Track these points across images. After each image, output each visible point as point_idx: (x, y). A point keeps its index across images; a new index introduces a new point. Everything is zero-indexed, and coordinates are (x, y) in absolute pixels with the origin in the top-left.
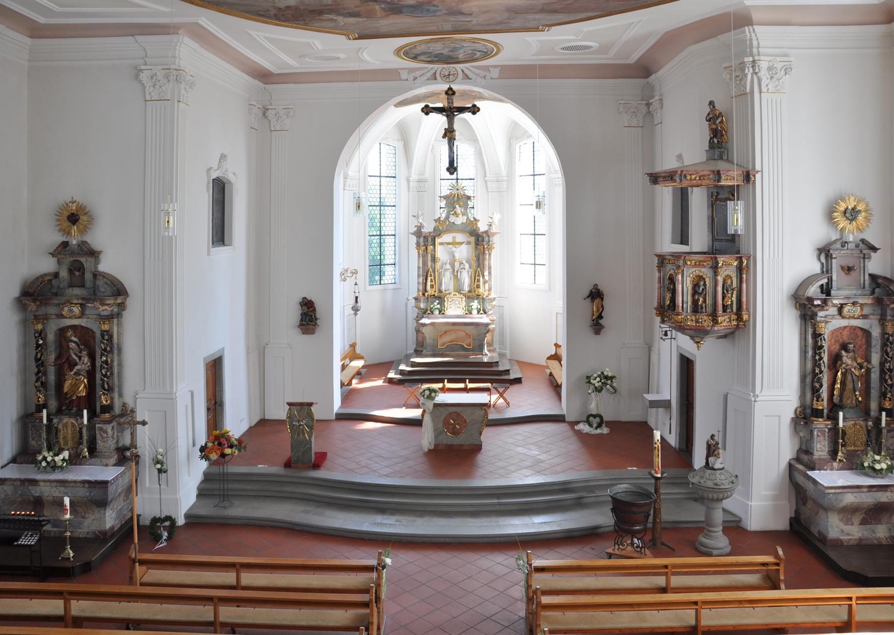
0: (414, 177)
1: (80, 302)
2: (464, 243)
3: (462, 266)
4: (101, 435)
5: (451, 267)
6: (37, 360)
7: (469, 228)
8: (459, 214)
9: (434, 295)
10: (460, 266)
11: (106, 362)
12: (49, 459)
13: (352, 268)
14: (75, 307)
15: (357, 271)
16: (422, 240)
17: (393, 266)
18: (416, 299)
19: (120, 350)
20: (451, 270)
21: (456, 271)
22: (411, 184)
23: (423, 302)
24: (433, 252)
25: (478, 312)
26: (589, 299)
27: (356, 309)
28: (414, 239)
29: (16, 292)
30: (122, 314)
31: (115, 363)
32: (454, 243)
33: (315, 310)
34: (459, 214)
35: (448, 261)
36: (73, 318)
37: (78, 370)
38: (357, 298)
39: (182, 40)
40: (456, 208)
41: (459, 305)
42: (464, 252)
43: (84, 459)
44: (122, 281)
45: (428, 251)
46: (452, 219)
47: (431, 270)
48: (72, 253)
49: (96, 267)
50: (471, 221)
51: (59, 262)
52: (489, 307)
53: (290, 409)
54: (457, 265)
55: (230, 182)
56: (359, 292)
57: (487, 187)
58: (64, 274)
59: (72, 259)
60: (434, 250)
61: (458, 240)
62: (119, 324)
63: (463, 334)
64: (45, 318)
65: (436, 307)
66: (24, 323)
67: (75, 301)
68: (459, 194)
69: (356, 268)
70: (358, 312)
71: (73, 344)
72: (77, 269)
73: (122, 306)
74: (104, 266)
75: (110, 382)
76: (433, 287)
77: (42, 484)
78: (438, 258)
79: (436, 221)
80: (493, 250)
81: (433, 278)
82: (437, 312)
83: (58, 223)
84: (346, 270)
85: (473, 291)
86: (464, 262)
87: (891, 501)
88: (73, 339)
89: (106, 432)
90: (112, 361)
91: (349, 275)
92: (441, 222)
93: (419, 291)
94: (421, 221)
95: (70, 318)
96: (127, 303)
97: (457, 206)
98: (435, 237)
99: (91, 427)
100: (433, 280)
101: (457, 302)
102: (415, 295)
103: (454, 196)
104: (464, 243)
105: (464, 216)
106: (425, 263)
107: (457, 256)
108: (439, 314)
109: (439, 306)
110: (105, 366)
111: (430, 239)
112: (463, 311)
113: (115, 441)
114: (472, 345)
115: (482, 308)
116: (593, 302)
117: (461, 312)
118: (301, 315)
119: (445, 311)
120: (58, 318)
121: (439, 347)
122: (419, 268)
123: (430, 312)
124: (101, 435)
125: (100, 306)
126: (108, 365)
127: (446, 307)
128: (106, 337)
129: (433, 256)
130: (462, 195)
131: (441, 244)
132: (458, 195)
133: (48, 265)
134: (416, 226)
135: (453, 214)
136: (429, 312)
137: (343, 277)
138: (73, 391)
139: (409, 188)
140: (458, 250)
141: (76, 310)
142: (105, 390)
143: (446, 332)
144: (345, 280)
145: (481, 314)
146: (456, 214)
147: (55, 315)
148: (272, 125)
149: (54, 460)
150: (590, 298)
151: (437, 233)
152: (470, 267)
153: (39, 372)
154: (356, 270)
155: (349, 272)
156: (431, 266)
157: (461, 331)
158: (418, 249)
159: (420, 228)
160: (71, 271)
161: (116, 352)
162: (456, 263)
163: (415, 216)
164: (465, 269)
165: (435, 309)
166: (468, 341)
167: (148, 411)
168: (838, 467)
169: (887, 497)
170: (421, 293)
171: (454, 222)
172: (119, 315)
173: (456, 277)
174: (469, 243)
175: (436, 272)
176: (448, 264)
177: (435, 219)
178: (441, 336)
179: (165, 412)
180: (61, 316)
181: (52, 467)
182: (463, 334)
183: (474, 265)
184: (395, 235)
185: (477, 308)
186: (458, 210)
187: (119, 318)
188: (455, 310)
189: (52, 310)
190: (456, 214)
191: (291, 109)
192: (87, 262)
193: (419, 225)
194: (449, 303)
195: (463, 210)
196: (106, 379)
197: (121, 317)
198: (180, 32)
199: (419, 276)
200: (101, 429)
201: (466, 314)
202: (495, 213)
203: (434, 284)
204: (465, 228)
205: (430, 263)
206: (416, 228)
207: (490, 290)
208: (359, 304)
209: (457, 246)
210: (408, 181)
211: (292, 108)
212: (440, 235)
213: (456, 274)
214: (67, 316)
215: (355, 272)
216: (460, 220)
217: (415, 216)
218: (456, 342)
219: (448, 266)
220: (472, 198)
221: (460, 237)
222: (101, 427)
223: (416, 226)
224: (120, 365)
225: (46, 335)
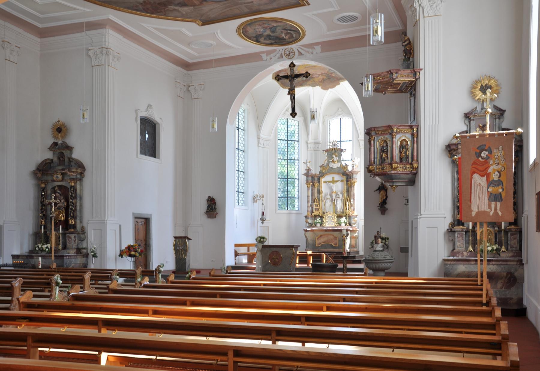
0: (311, 140)
1: (61, 172)
2: (338, 181)
3: (337, 196)
4: (69, 240)
5: (331, 197)
6: (42, 203)
7: (342, 171)
8: (336, 161)
10: (336, 196)
11: (72, 203)
12: (40, 246)
13: (260, 193)
14: (59, 175)
15: (264, 196)
16: (310, 178)
17: (297, 199)
18: (306, 217)
19: (81, 198)
20: (330, 199)
22: (309, 145)
23: (311, 219)
24: (319, 188)
25: (346, 225)
26: (378, 191)
27: (263, 220)
28: (304, 178)
29: (33, 168)
30: (82, 180)
31: (78, 204)
32: (334, 182)
33: (215, 203)
35: (329, 193)
36: (58, 182)
37: (59, 206)
38: (263, 213)
39: (108, 31)
40: (333, 157)
41: (332, 220)
42: (339, 187)
43: (59, 251)
44: (82, 162)
45: (315, 186)
46: (331, 165)
47: (317, 198)
48: (59, 148)
49: (71, 156)
50: (343, 166)
51: (54, 154)
53: (175, 240)
54: (334, 195)
55: (158, 124)
56: (265, 209)
57: (360, 145)
58: (56, 159)
59: (59, 152)
60: (319, 186)
61: (335, 179)
62: (81, 185)
63: (332, 237)
64: (46, 183)
65: (318, 222)
66: (38, 185)
67: (59, 172)
68: (336, 149)
69: (262, 194)
70: (264, 222)
71: (58, 194)
72: (61, 156)
73: (82, 174)
74: (75, 156)
75: (75, 214)
76: (318, 210)
77: (35, 257)
78: (322, 191)
79: (321, 167)
80: (356, 183)
81: (318, 204)
82: (318, 225)
83: (53, 133)
84: (257, 196)
85: (344, 212)
86: (339, 193)
87: (493, 271)
88: (58, 191)
89: (71, 238)
90: (76, 203)
91: (259, 198)
92: (324, 167)
93: (308, 211)
94: (308, 166)
95: (58, 181)
96: (85, 174)
97: (334, 156)
98: (320, 178)
99: (64, 235)
100: (319, 206)
101: (332, 218)
102: (306, 214)
103: (332, 150)
104: (338, 181)
105: (338, 163)
106: (313, 194)
107: (334, 189)
109: (319, 221)
110: (72, 204)
111: (316, 179)
113: (76, 244)
115: (348, 222)
116: (380, 193)
117: (334, 225)
118: (207, 207)
120: (53, 182)
121: (317, 246)
122: (308, 197)
123: (314, 225)
124: (69, 240)
125: (69, 172)
126: (75, 205)
127: (324, 222)
128: (72, 189)
129: (319, 190)
131: (325, 182)
132: (335, 149)
133: (49, 155)
134: (306, 170)
135: (332, 162)
136: (314, 225)
137: (255, 200)
138: (57, 218)
139: (308, 149)
140: (335, 185)
141: (60, 176)
142: (72, 217)
143: (321, 236)
144: (256, 202)
145: (348, 226)
146: (333, 161)
147: (51, 180)
148: (192, 96)
149: (42, 247)
150: (378, 191)
151: (322, 175)
152: (343, 197)
153: (42, 209)
154: (263, 195)
155: (259, 197)
156: (318, 196)
157: (331, 235)
158: (307, 185)
159: (308, 170)
160: (59, 158)
161: (78, 199)
162: (333, 194)
163: (305, 163)
164: (339, 198)
165: (317, 222)
166: (336, 241)
167: (93, 230)
168: (467, 255)
169: (490, 268)
170: (309, 213)
171: (332, 167)
172: (81, 180)
173: (334, 203)
174: (342, 181)
176: (328, 195)
177: (320, 165)
179: (101, 230)
180: (53, 181)
181: (41, 250)
182: (332, 237)
183: (345, 195)
184: (298, 179)
185: (345, 222)
186: (335, 159)
187: (81, 182)
188: (330, 223)
189: (49, 178)
190: (333, 161)
191: (202, 85)
192: (66, 153)
193: (308, 168)
194: (326, 219)
195: (338, 159)
196: (72, 211)
197: (82, 181)
198: (107, 27)
199: (308, 202)
200: (69, 237)
201: (338, 226)
202: (356, 158)
203: (319, 208)
205: (316, 195)
206: (306, 171)
207: (354, 210)
208: (265, 217)
209: (335, 183)
210: (307, 144)
211: (203, 85)
213: (334, 201)
214: (56, 180)
215: (262, 197)
216: (335, 166)
217: (305, 163)
218: (328, 242)
219: (329, 197)
220: (344, 150)
221: (337, 177)
222: (69, 236)
223: (306, 170)
224: (81, 206)
225: (47, 191)
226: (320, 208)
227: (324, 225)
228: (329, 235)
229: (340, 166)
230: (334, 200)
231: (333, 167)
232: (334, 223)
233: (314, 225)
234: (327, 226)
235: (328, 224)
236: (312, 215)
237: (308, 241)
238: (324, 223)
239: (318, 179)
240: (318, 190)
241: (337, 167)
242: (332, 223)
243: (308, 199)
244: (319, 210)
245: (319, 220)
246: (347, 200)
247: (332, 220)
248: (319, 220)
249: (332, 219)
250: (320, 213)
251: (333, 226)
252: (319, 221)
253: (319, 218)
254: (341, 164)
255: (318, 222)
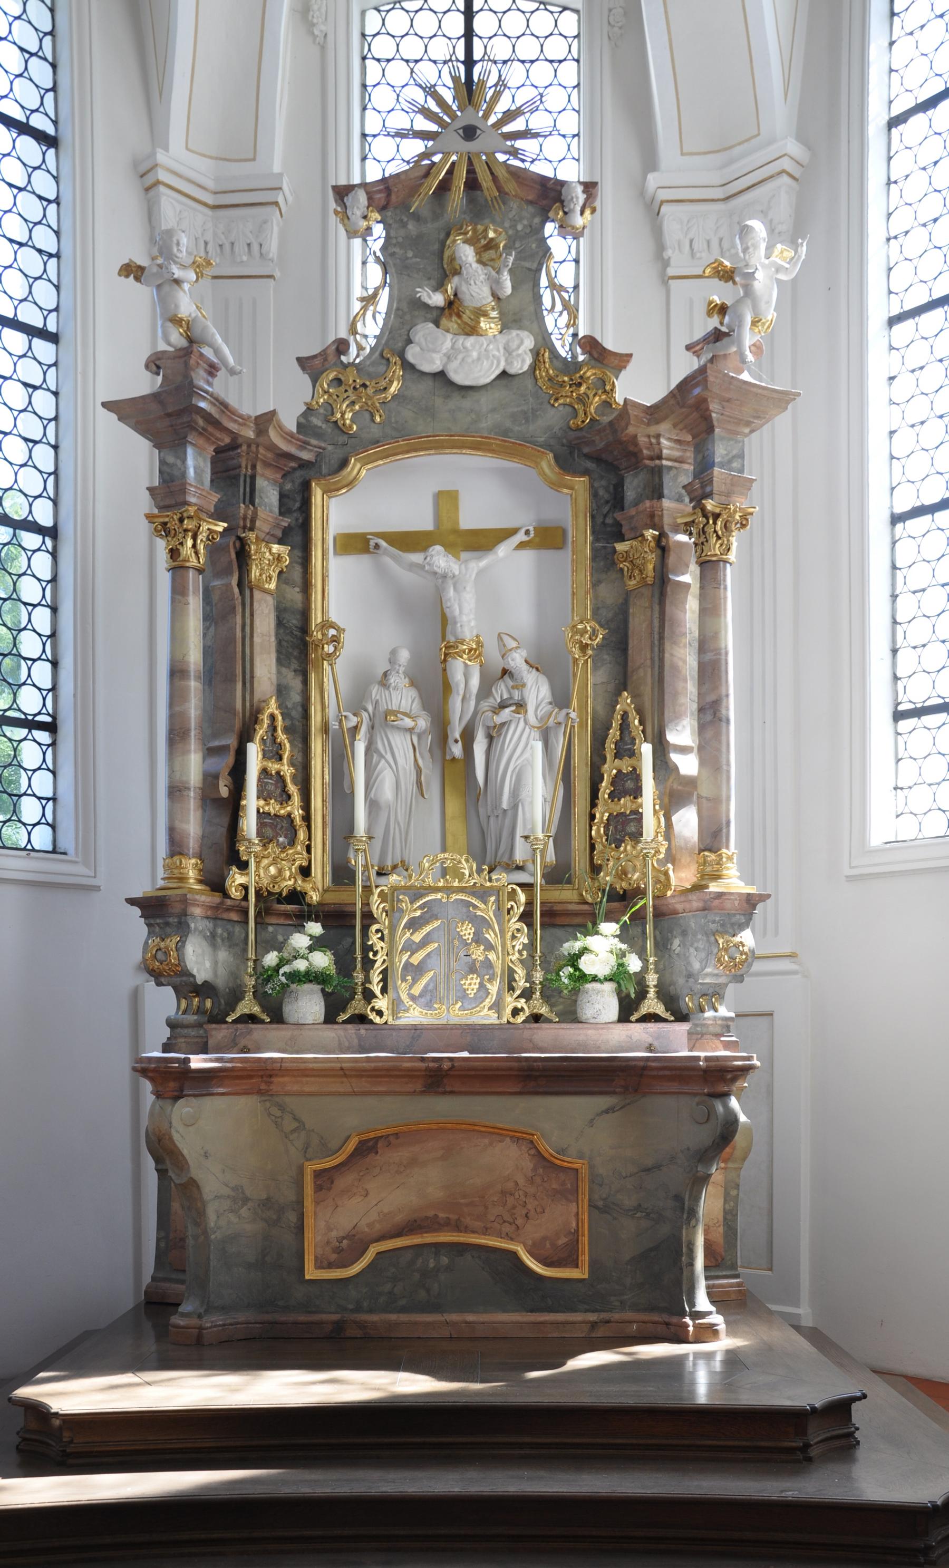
2: (513, 532)
3: (501, 691)
5: (426, 705)
8: (481, 313)
9: (296, 896)
10: (485, 691)
21: (456, 732)
23: (212, 939)
24: (294, 595)
25: (628, 1009)
34: (481, 313)
35: (404, 656)
41: (478, 953)
45: (255, 572)
47: (273, 707)
52: (710, 974)
76: (292, 842)
78: (327, 624)
81: (287, 771)
86: (517, 660)
93: (176, 847)
97: (467, 253)
98: (306, 489)
100: (292, 789)
101: (467, 931)
103: (445, 187)
108: (330, 1018)
109: (322, 960)
112: (510, 1002)
114: (585, 1259)
115: (652, 979)
117: (497, 1006)
119: (369, 996)
121: (311, 1273)
127: (378, 966)
129: (294, 621)
130: (501, 173)
135: (437, 316)
136: (248, 1005)
145: (652, 1018)
156: (281, 691)
157: (497, 1133)
162: (457, 668)
164: (520, 706)
165: (295, 977)
170: (191, 869)
175: (316, 745)
176: (398, 680)
178: (324, 1179)
185: (618, 976)
194: (403, 937)
201: (536, 1018)
203: (298, 813)
204: (528, 417)
212: (344, 463)
213: (457, 750)
218: (458, 1227)
226: (307, 818)
227: (381, 1003)
228: (472, 1129)
229: (529, 360)
230: (456, 732)
231: (459, 378)
232: (494, 988)
233: (248, 1005)
234: (415, 1015)
235: (428, 998)
236: (217, 885)
237: (197, 1212)
238: (377, 990)
239: (282, 496)
240: (280, 623)
241: (504, 374)
242: (472, 984)
243: (176, 697)
244: (302, 835)
245: (317, 944)
246: (614, 733)
247: (478, 953)
248: (317, 944)
249: (478, 939)
250: (305, 872)
251: (485, 1016)
252: (322, 960)
253: (315, 928)
254: (544, 343)
255: (311, 977)
